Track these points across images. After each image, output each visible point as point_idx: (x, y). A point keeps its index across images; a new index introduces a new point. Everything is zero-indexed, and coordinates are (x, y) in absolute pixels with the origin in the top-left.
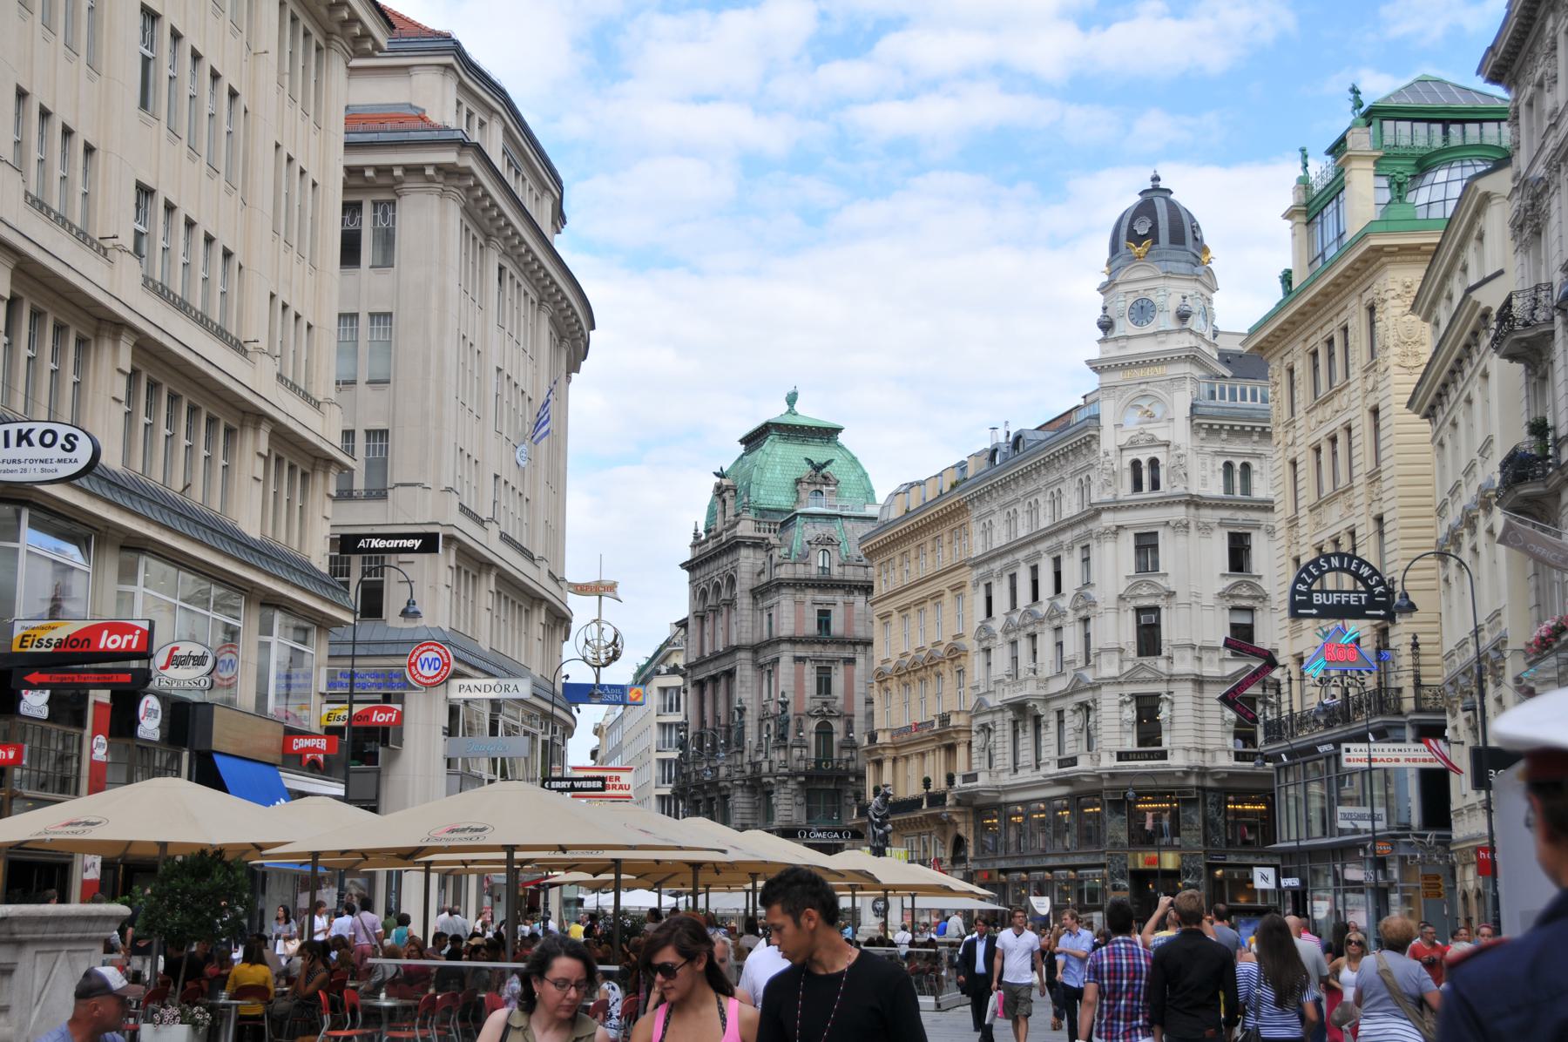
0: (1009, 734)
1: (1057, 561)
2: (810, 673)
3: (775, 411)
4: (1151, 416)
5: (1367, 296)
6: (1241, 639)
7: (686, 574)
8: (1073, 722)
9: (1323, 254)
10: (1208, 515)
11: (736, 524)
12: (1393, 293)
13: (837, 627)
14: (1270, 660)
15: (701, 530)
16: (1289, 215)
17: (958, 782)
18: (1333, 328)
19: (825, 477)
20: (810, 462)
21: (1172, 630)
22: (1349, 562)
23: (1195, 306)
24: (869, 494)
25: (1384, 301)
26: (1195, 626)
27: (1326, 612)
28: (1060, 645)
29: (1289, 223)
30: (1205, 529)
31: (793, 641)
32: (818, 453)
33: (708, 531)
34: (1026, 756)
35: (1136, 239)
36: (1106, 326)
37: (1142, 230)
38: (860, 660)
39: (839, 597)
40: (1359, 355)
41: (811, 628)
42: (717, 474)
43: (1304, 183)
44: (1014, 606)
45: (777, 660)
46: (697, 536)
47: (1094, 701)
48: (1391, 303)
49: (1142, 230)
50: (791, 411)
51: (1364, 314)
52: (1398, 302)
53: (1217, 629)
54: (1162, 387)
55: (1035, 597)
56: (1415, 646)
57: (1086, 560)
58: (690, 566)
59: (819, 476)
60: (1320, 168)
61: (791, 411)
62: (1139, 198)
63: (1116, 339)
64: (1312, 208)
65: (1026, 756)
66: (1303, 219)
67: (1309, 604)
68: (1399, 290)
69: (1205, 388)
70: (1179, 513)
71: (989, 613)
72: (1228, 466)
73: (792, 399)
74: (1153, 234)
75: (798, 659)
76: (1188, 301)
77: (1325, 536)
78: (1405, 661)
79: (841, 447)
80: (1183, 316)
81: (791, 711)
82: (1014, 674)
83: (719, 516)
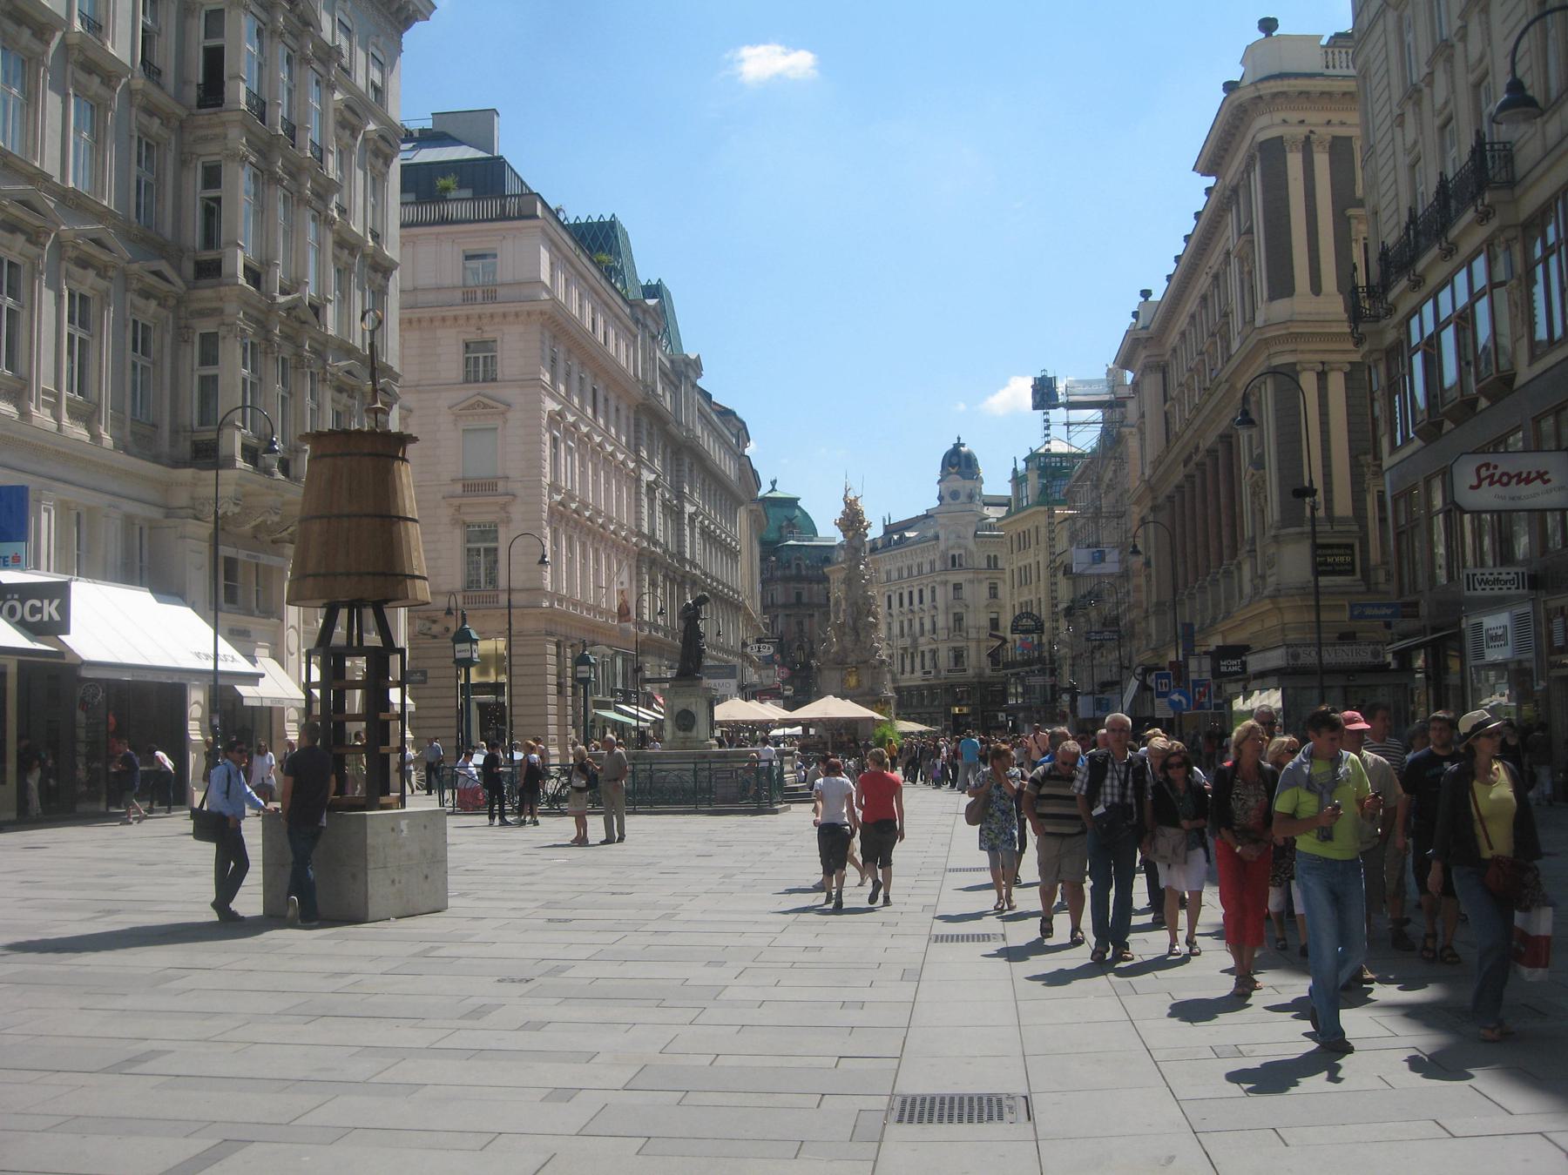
1: (921, 591)
6: (995, 624)
8: (928, 656)
10: (982, 576)
13: (805, 599)
14: (1005, 641)
21: (969, 620)
22: (1029, 615)
26: (978, 620)
27: (1022, 632)
28: (922, 625)
30: (980, 581)
31: (785, 606)
34: (908, 668)
36: (940, 498)
37: (955, 460)
39: (806, 586)
40: (1033, 541)
41: (793, 600)
44: (901, 605)
49: (955, 460)
50: (773, 489)
53: (984, 621)
55: (911, 603)
57: (933, 591)
60: (1021, 466)
61: (773, 489)
64: (1018, 480)
65: (908, 668)
70: (971, 576)
73: (774, 483)
74: (959, 464)
77: (1023, 599)
78: (1046, 647)
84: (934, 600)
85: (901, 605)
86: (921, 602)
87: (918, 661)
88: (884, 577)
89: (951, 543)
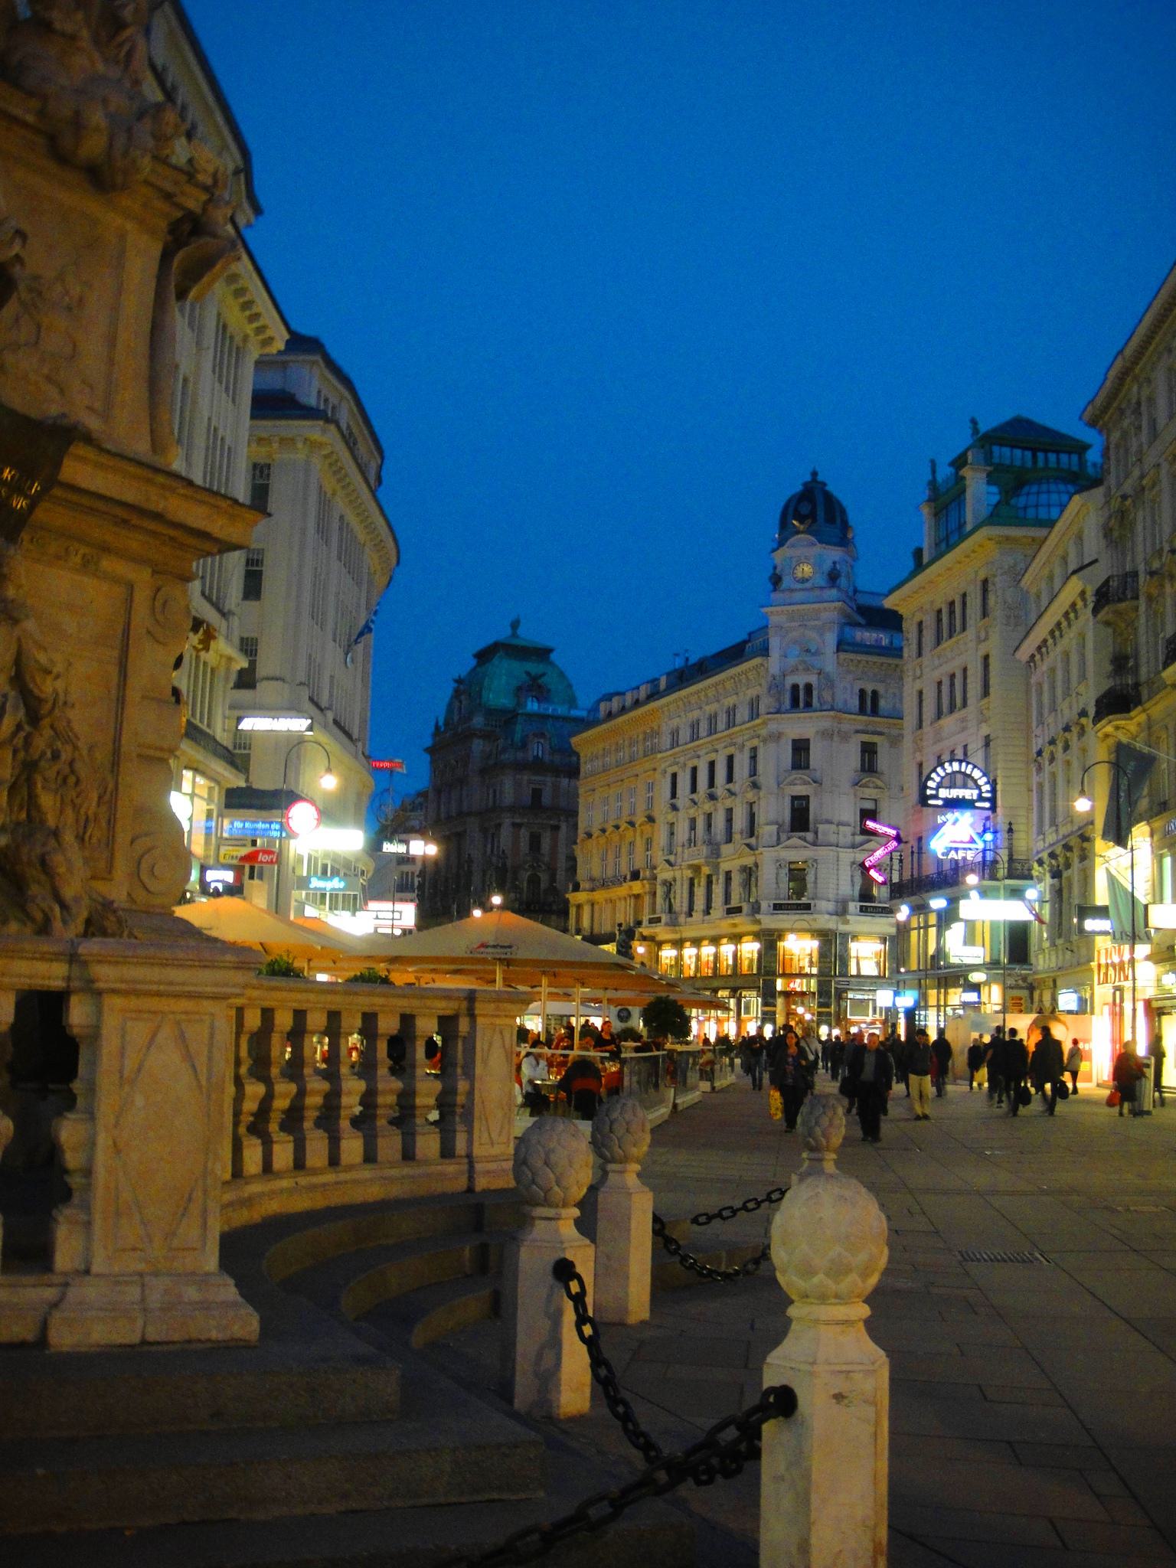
0: (686, 886)
1: (730, 759)
2: (524, 834)
3: (503, 633)
4: (808, 651)
7: (427, 757)
8: (737, 879)
11: (470, 719)
13: (546, 800)
15: (441, 723)
17: (645, 922)
19: (540, 687)
20: (528, 673)
24: (572, 702)
28: (729, 820)
30: (845, 737)
31: (512, 809)
32: (534, 668)
33: (446, 724)
38: (564, 827)
41: (527, 799)
42: (456, 681)
43: (933, 484)
44: (694, 790)
45: (500, 825)
46: (437, 727)
47: (756, 865)
50: (514, 635)
56: (1010, 830)
58: (430, 751)
59: (535, 688)
61: (514, 635)
67: (936, 797)
71: (674, 795)
72: (862, 692)
73: (515, 625)
74: (812, 515)
75: (514, 825)
79: (552, 664)
81: (509, 863)
82: (692, 842)
83: (456, 712)
84: (753, 772)
85: (694, 790)
86: (730, 778)
87: (718, 890)
88: (666, 740)
89: (792, 661)
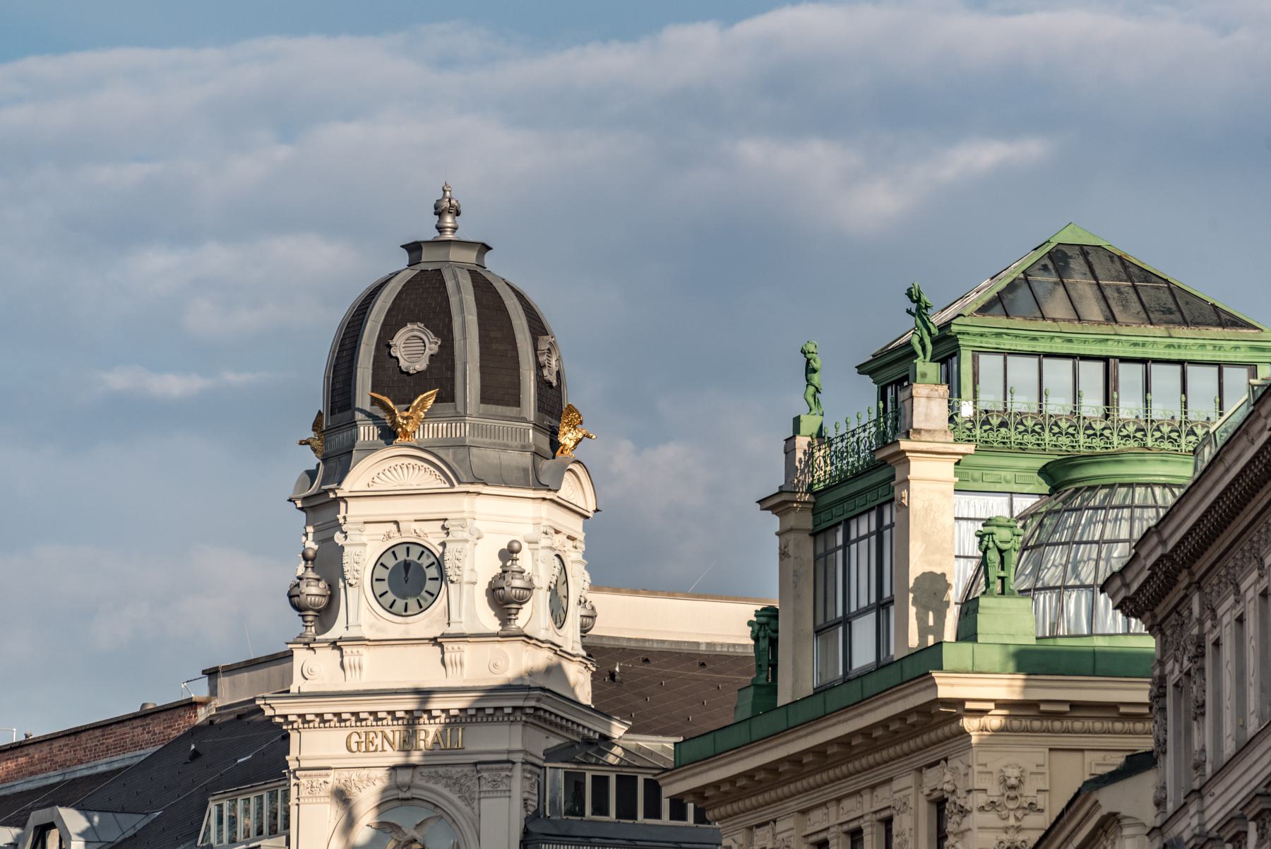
5: (933, 779)
9: (846, 621)
12: (981, 799)
16: (776, 504)
18: (862, 808)
23: (536, 567)
25: (964, 812)
29: (774, 522)
35: (397, 385)
48: (976, 819)
51: (924, 810)
52: (991, 818)
54: (454, 783)
62: (401, 260)
63: (334, 644)
66: (807, 521)
68: (995, 791)
69: (556, 775)
74: (440, 378)
76: (524, 560)
80: (504, 601)
